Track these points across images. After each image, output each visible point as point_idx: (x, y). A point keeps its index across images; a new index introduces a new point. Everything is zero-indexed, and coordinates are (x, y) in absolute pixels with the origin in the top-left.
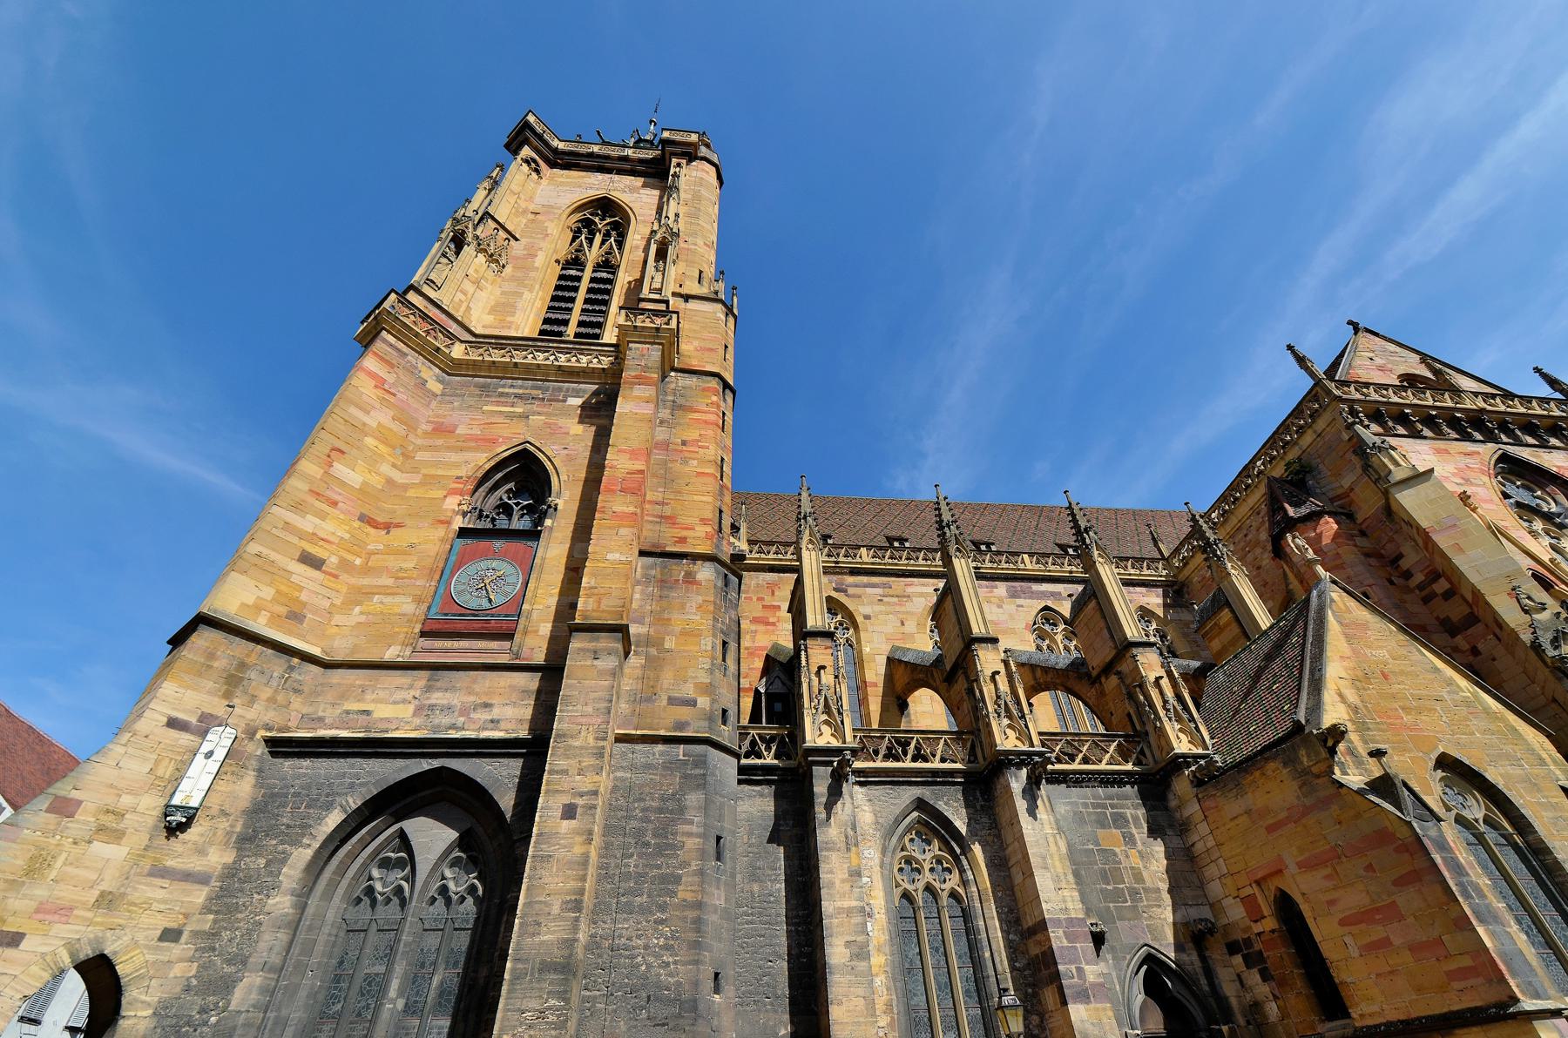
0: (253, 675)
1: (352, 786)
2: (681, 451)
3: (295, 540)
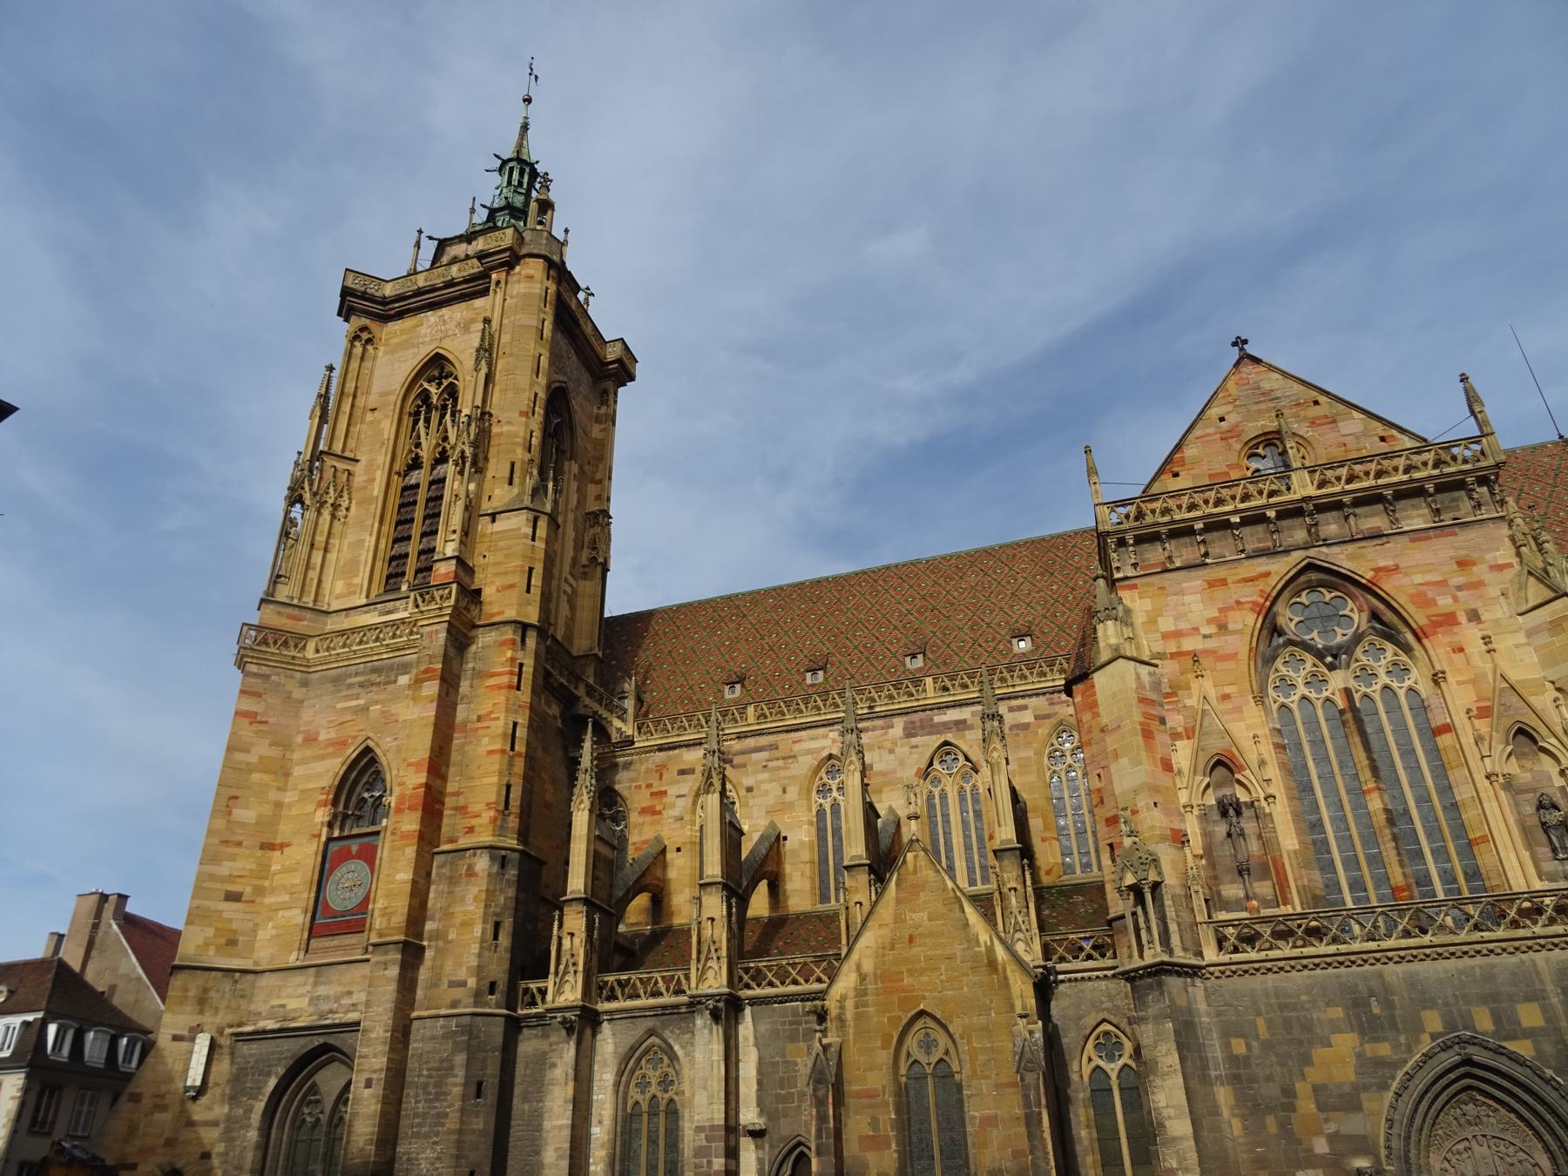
0: (213, 994)
1: (279, 1059)
2: (477, 729)
3: (218, 886)
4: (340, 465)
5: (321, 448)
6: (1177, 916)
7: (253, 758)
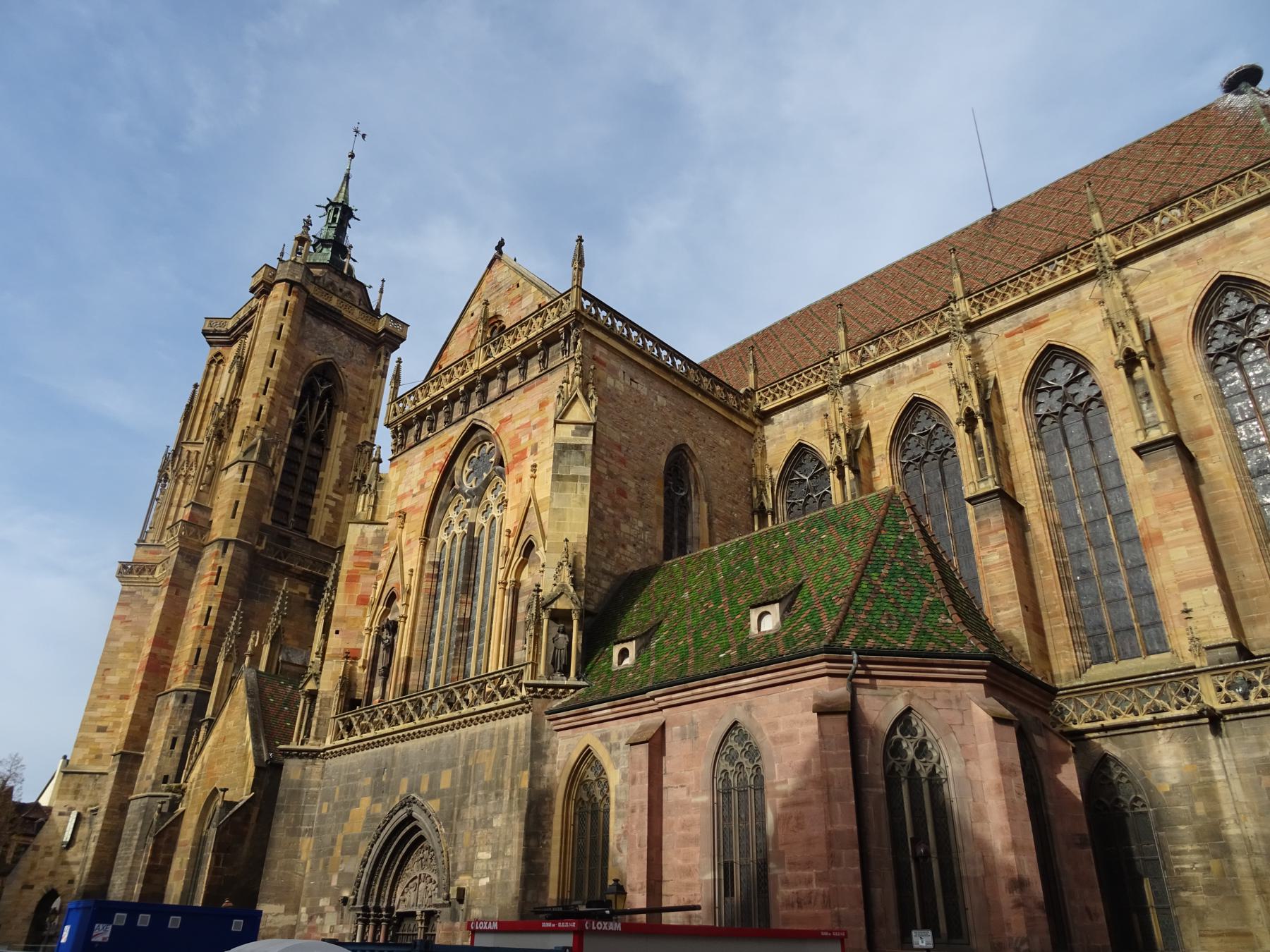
0: (83, 788)
3: (94, 723)
4: (192, 449)
5: (185, 440)
6: (320, 714)
7: (120, 644)
